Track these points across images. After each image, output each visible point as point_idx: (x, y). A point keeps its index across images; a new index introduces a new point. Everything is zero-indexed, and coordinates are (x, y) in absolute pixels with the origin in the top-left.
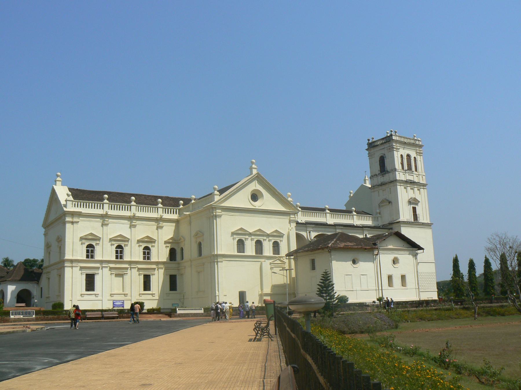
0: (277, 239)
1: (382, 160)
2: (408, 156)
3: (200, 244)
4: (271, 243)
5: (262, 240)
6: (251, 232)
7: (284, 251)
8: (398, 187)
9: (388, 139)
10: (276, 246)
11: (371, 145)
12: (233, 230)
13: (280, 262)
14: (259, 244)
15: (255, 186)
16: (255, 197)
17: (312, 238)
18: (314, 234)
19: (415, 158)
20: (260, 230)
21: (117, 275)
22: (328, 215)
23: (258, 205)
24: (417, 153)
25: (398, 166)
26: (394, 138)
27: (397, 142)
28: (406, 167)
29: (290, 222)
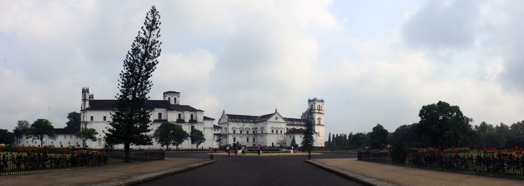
1: (312, 106)
3: (262, 130)
7: (283, 133)
8: (316, 115)
9: (314, 100)
10: (281, 132)
11: (310, 101)
14: (277, 131)
16: (276, 118)
19: (321, 106)
21: (241, 138)
23: (277, 121)
25: (316, 108)
26: (316, 100)
28: (318, 109)
29: (285, 125)
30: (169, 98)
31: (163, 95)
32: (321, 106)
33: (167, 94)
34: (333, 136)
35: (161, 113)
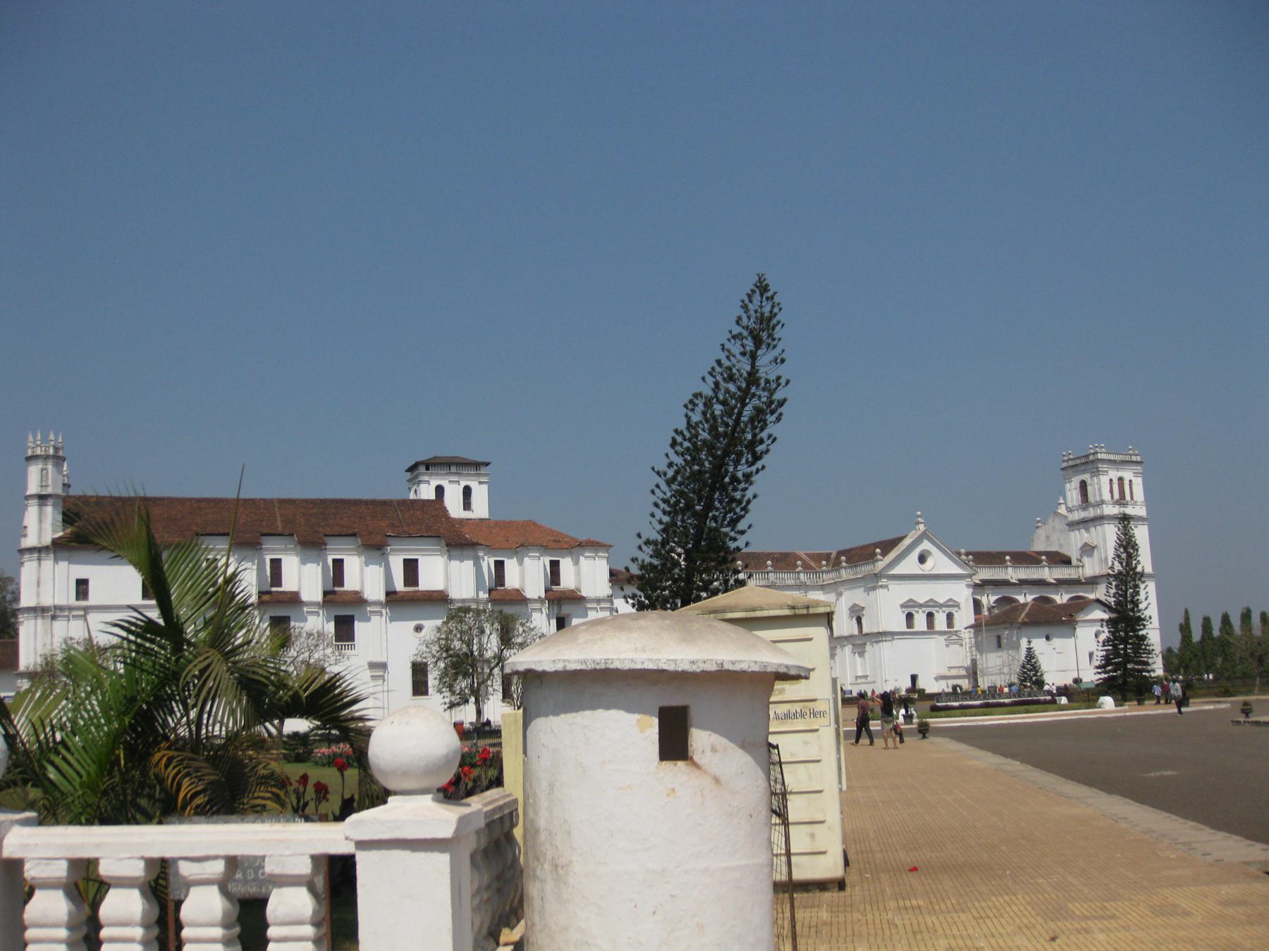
0: (953, 610)
2: (1121, 480)
3: (859, 620)
4: (945, 615)
5: (934, 612)
6: (921, 602)
12: (901, 603)
13: (956, 638)
14: (930, 616)
15: (926, 545)
17: (991, 603)
18: (993, 598)
19: (1130, 481)
20: (931, 600)
22: (1010, 570)
23: (928, 567)
24: (1134, 473)
27: (1103, 461)
28: (1117, 496)
29: (968, 586)
30: (440, 490)
31: (409, 475)
32: (1130, 481)
33: (427, 469)
34: (1207, 624)
35: (342, 560)
